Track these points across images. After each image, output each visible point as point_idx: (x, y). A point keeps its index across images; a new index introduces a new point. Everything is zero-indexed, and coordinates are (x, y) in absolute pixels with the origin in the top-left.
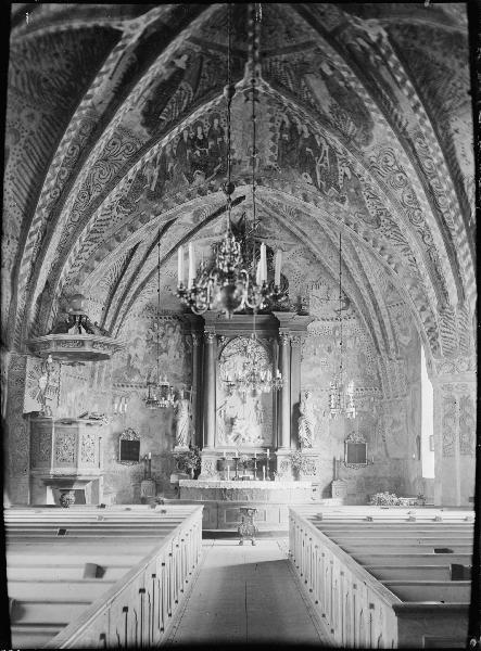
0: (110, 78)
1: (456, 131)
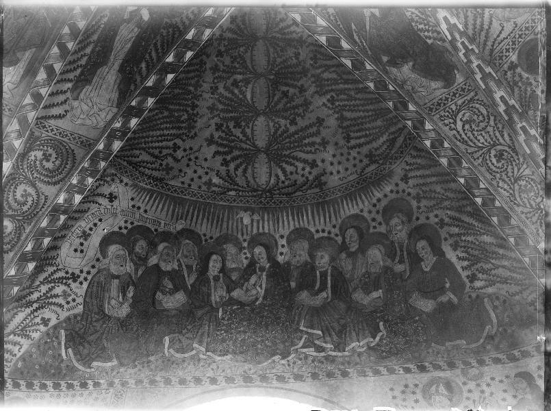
1: (112, 198)
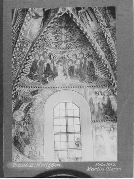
0: (92, 21)
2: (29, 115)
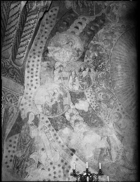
2: (96, 46)
